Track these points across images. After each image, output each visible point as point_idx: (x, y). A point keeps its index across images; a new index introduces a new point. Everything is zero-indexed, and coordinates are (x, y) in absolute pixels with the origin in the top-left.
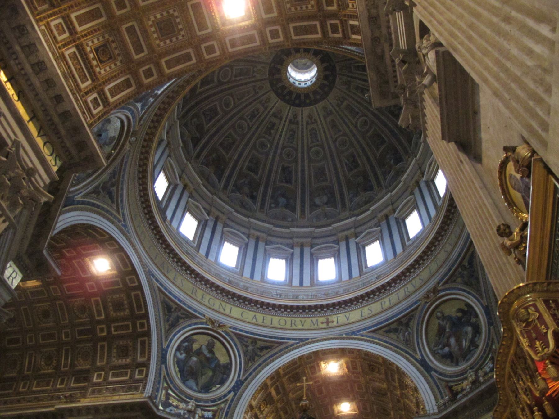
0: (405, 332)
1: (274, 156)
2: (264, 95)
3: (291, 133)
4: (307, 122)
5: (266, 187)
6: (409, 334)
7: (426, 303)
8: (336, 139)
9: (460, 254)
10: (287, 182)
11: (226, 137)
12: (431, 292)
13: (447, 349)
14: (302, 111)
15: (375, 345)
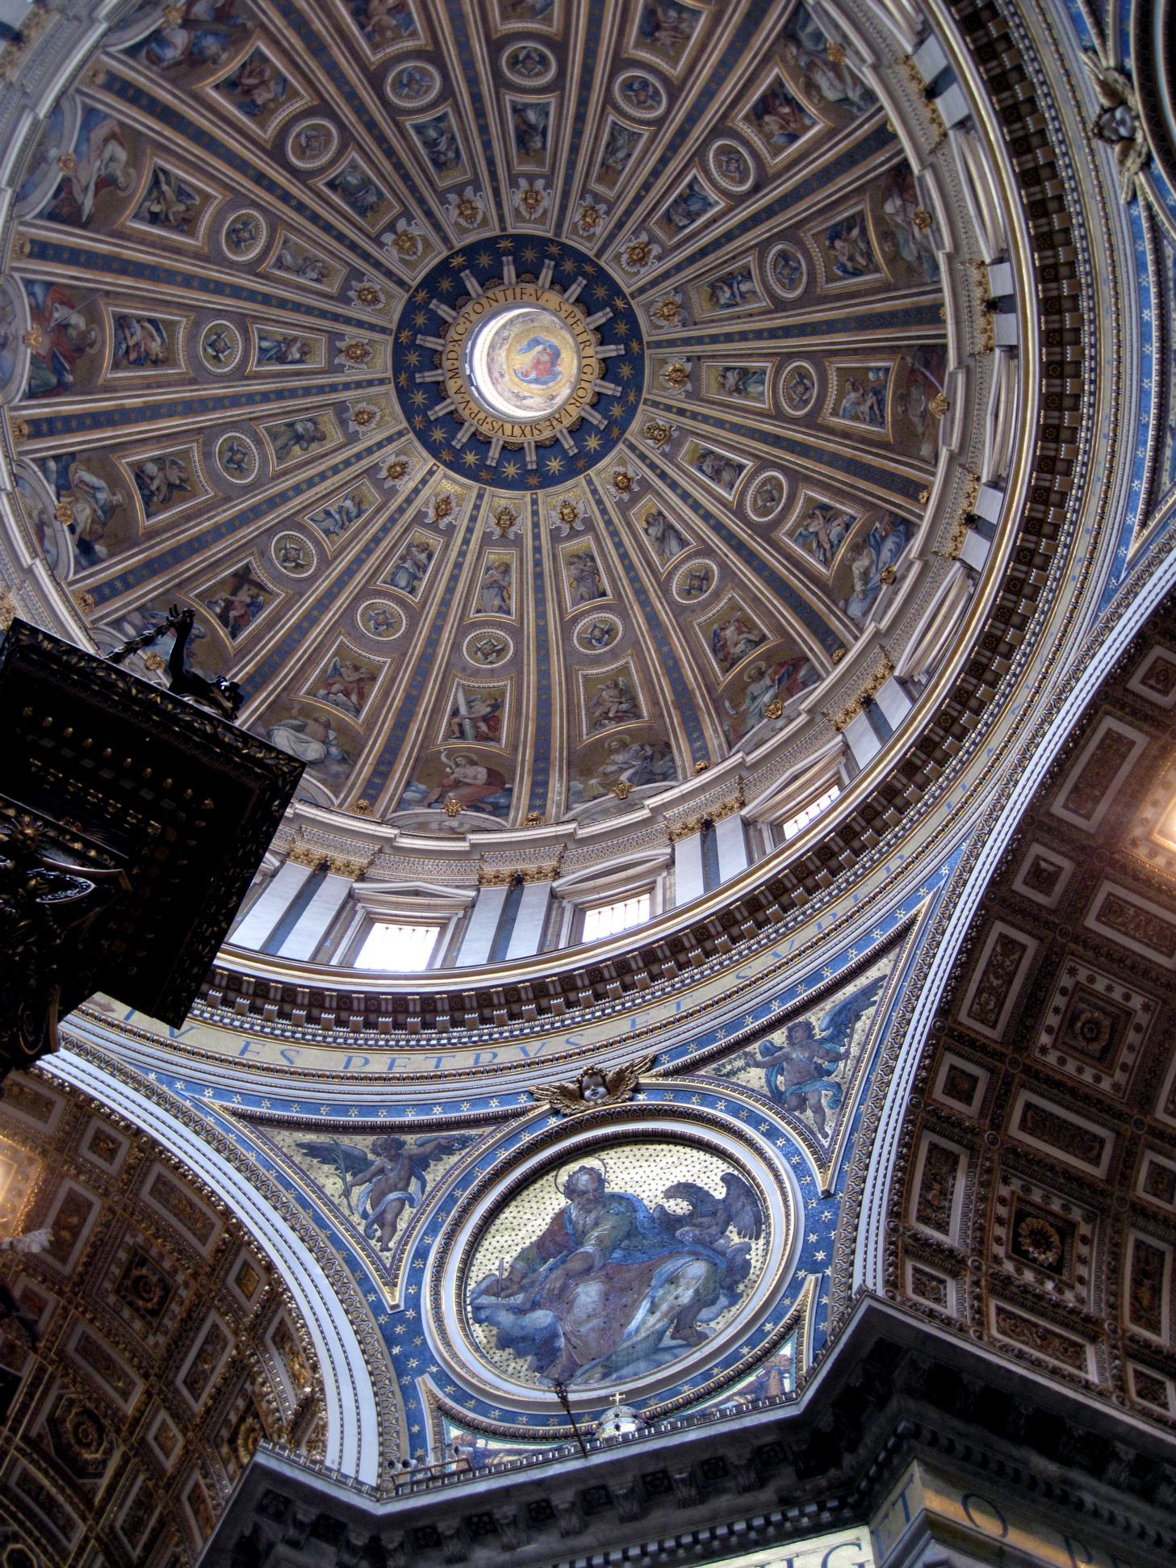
0: (395, 1188)
1: (243, 519)
2: (360, 324)
3: (348, 504)
4: (420, 516)
5: (152, 568)
6: (402, 1202)
7: (556, 1112)
8: (475, 625)
9: (816, 976)
10: (223, 618)
11: (152, 321)
12: (604, 1084)
13: (542, 1318)
14: (431, 473)
15: (229, 1168)
